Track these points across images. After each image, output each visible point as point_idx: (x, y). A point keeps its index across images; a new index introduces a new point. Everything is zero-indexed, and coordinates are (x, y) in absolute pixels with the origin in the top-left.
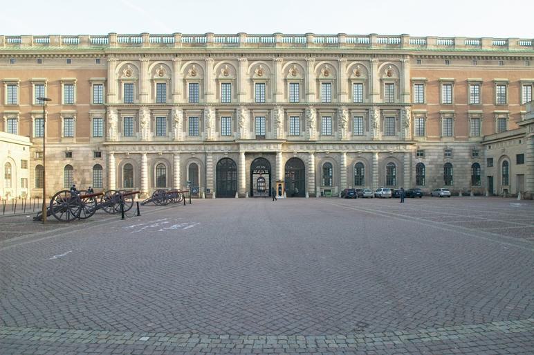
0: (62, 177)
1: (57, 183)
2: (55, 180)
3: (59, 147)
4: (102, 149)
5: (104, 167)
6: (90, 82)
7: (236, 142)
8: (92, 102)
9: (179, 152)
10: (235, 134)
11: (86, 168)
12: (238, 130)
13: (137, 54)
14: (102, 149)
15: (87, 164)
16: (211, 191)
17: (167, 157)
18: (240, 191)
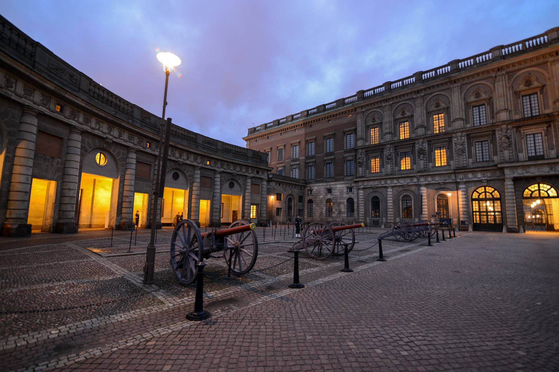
0: (325, 208)
1: (321, 213)
2: (320, 210)
3: (323, 185)
4: (353, 185)
5: (355, 200)
6: (344, 133)
7: (499, 166)
8: (345, 148)
9: (425, 183)
10: (495, 158)
11: (342, 201)
12: (498, 154)
13: (380, 102)
14: (353, 185)
15: (342, 198)
16: (466, 223)
17: (413, 188)
18: (508, 224)
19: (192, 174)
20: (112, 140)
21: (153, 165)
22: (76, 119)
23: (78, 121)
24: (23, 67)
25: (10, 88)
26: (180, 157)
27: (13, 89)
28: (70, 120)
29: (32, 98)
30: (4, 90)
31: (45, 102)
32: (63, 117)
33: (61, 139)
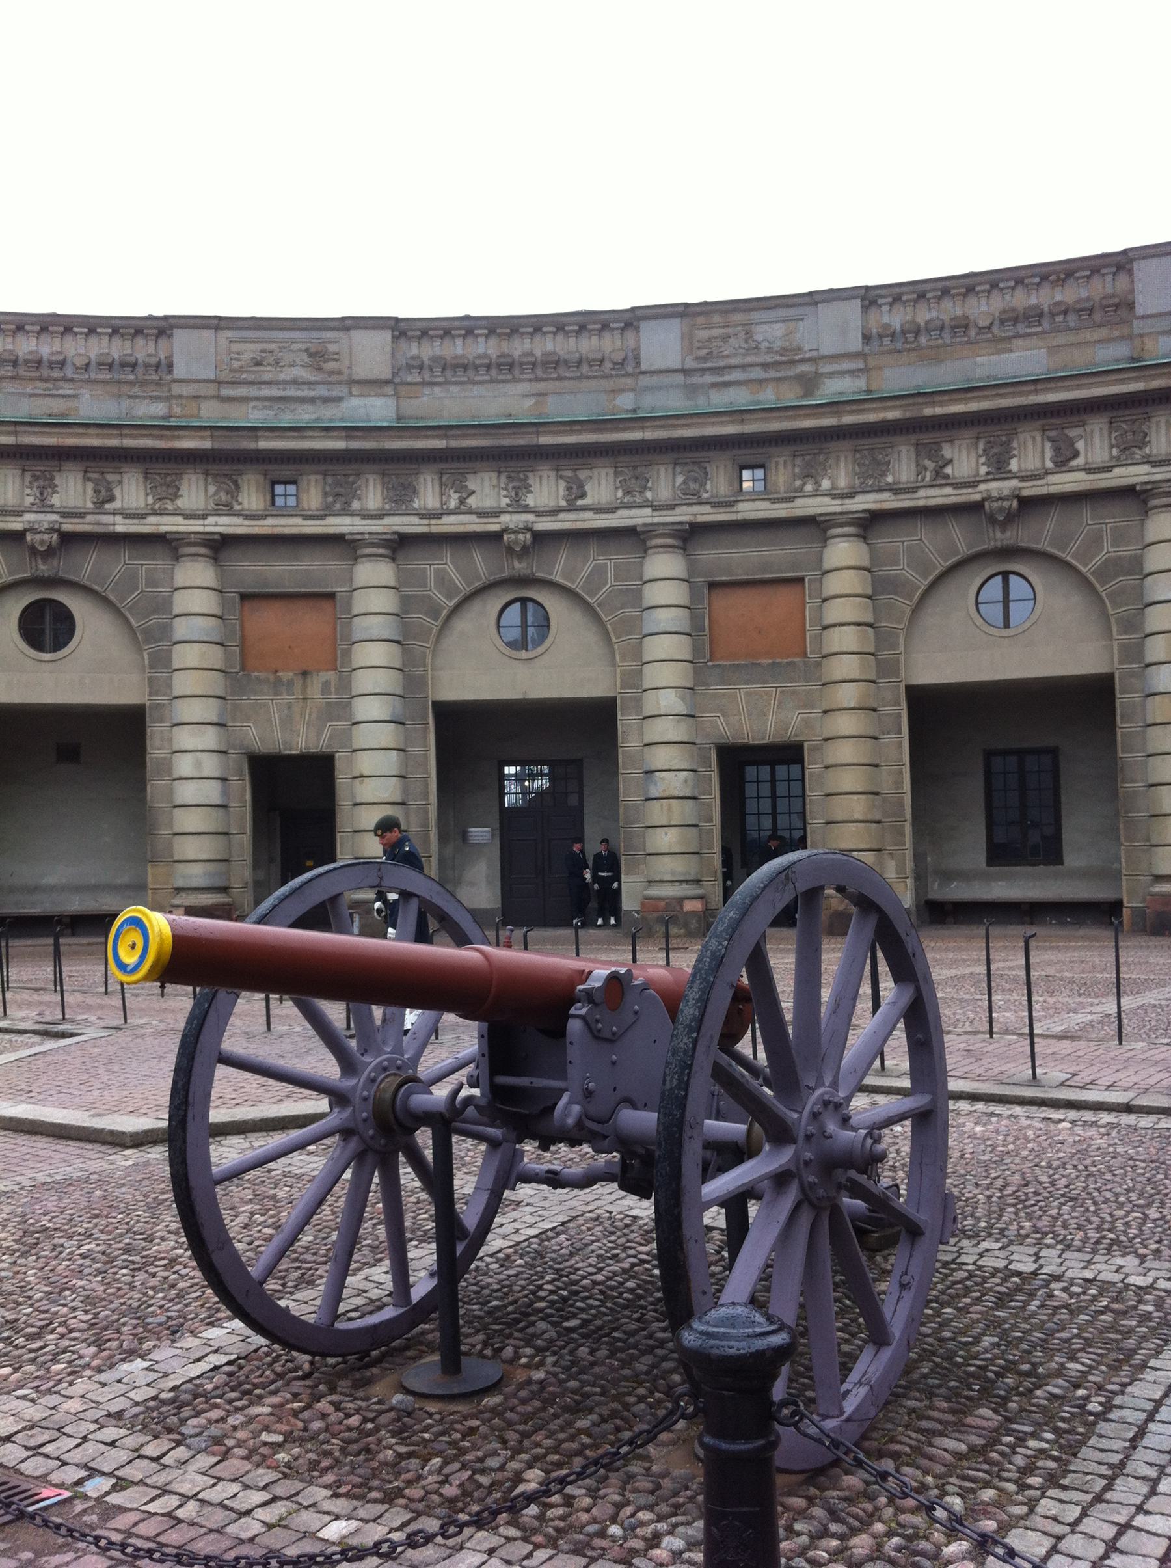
19: (1127, 551)
20: (528, 529)
21: (809, 575)
22: (356, 505)
23: (370, 510)
24: (92, 431)
25: (107, 506)
26: (999, 469)
27: (116, 505)
28: (331, 520)
29: (179, 503)
30: (89, 518)
31: (224, 497)
32: (298, 521)
33: (331, 596)
